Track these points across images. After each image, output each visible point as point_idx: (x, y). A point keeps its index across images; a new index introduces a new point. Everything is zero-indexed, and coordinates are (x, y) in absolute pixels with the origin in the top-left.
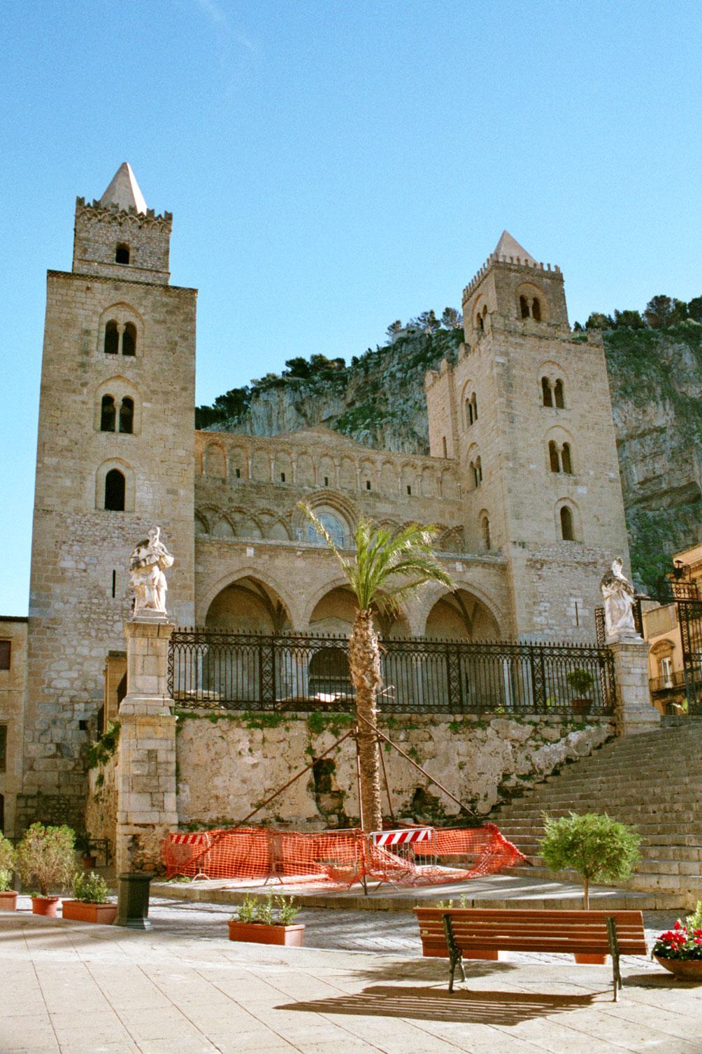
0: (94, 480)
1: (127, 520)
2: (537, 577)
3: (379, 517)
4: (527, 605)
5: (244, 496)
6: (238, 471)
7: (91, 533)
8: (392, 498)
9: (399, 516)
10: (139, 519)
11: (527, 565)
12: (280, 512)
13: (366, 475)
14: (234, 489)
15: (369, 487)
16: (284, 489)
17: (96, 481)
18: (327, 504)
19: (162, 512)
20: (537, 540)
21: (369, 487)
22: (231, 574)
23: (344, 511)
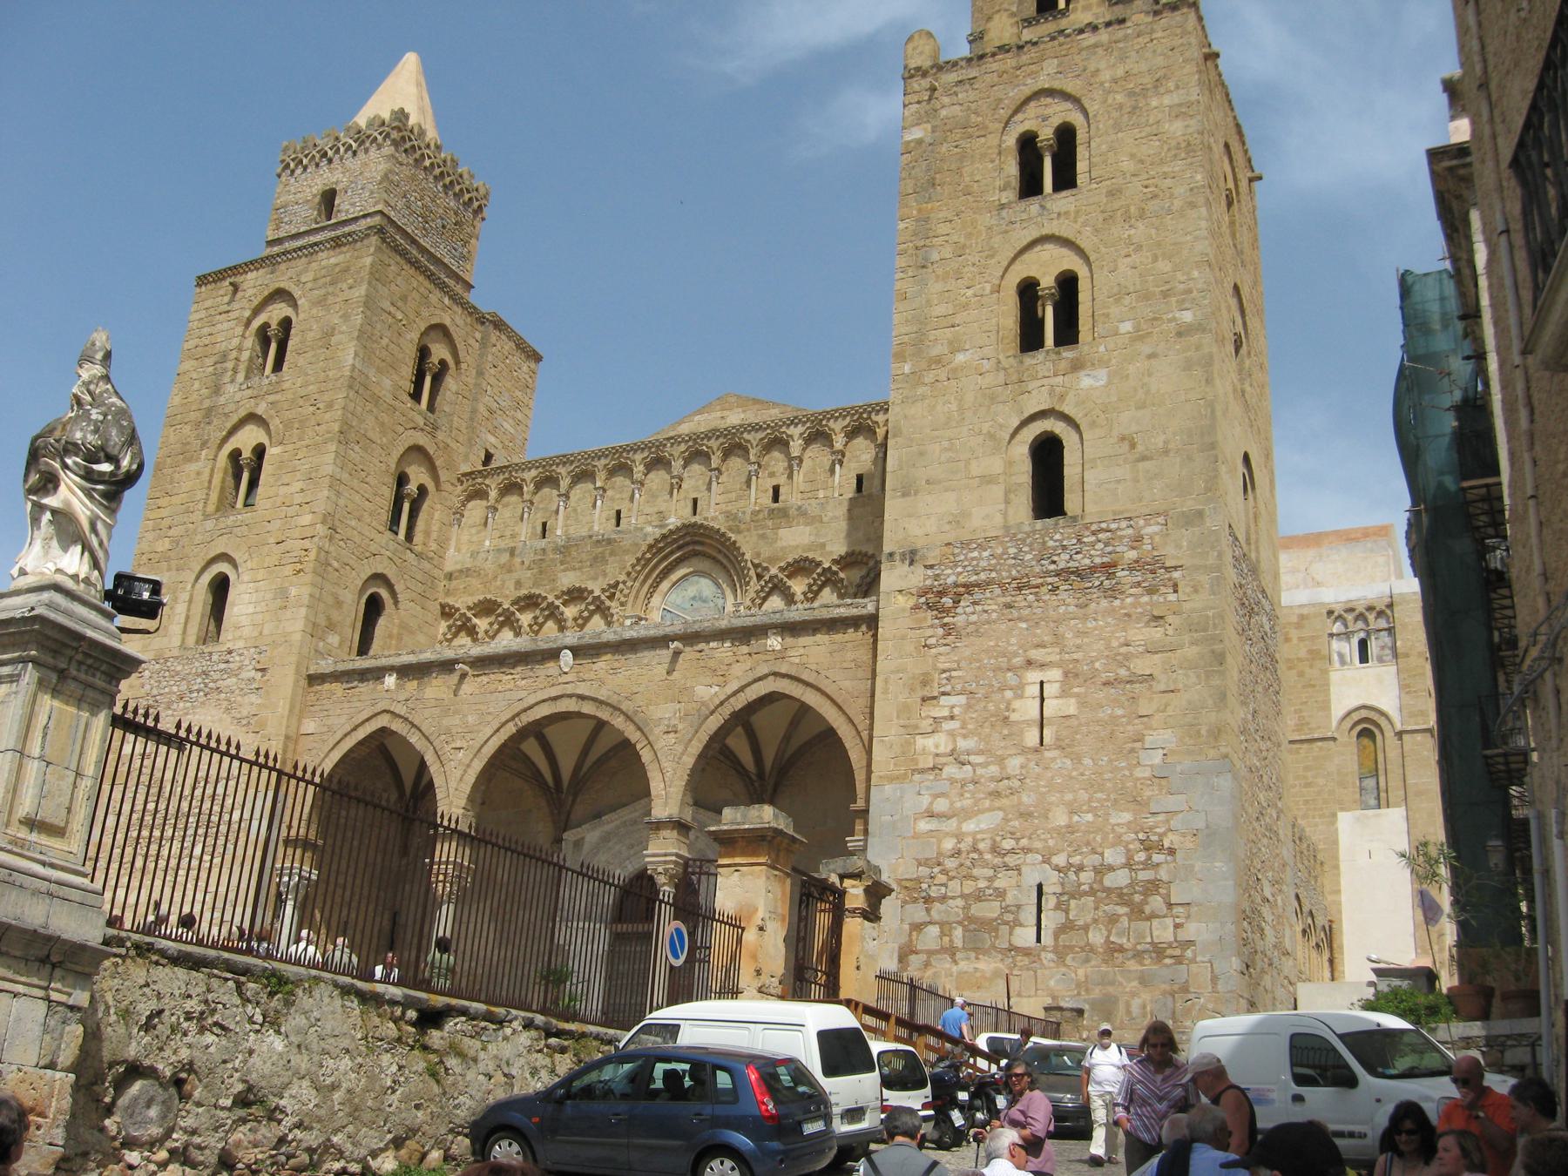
0: (187, 598)
1: (215, 657)
2: (940, 631)
3: (780, 560)
4: (904, 709)
5: (541, 572)
6: (544, 525)
7: (167, 690)
8: (813, 508)
9: (823, 546)
10: (230, 652)
11: (916, 607)
12: (596, 587)
13: (772, 475)
14: (527, 563)
15: (776, 498)
16: (609, 541)
17: (190, 601)
18: (696, 554)
19: (261, 634)
20: (950, 538)
21: (776, 498)
22: (355, 729)
23: (725, 561)
